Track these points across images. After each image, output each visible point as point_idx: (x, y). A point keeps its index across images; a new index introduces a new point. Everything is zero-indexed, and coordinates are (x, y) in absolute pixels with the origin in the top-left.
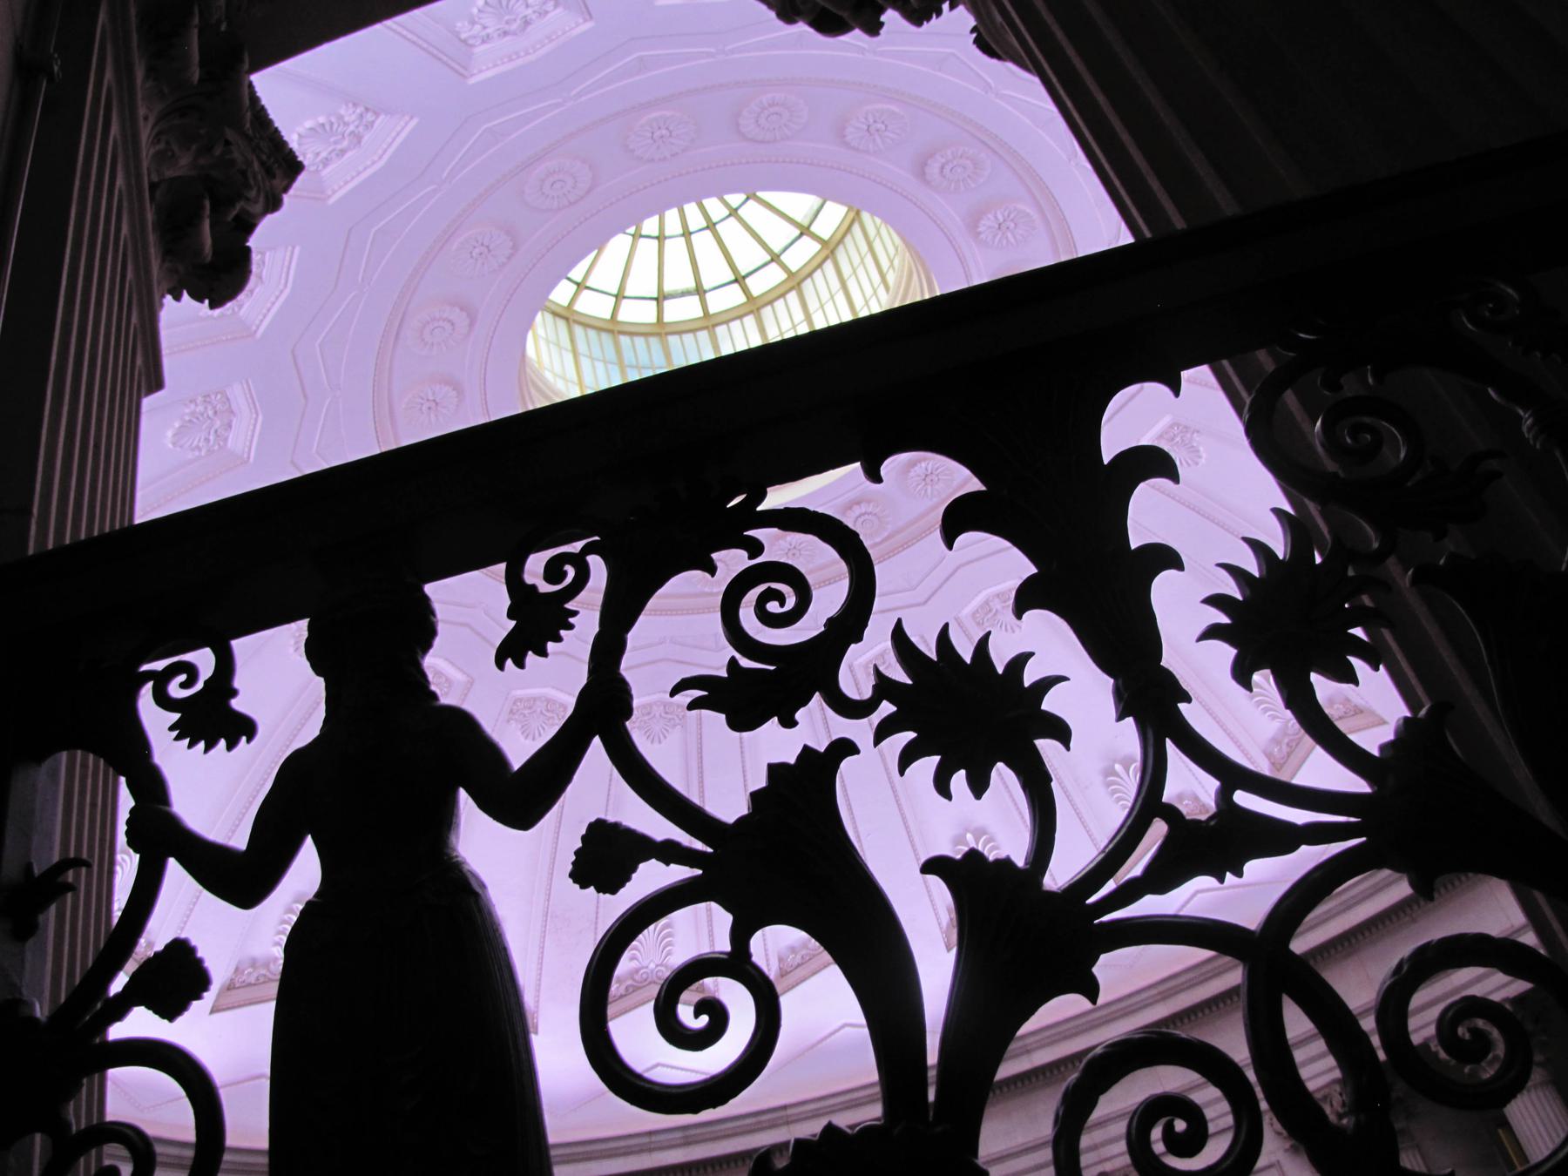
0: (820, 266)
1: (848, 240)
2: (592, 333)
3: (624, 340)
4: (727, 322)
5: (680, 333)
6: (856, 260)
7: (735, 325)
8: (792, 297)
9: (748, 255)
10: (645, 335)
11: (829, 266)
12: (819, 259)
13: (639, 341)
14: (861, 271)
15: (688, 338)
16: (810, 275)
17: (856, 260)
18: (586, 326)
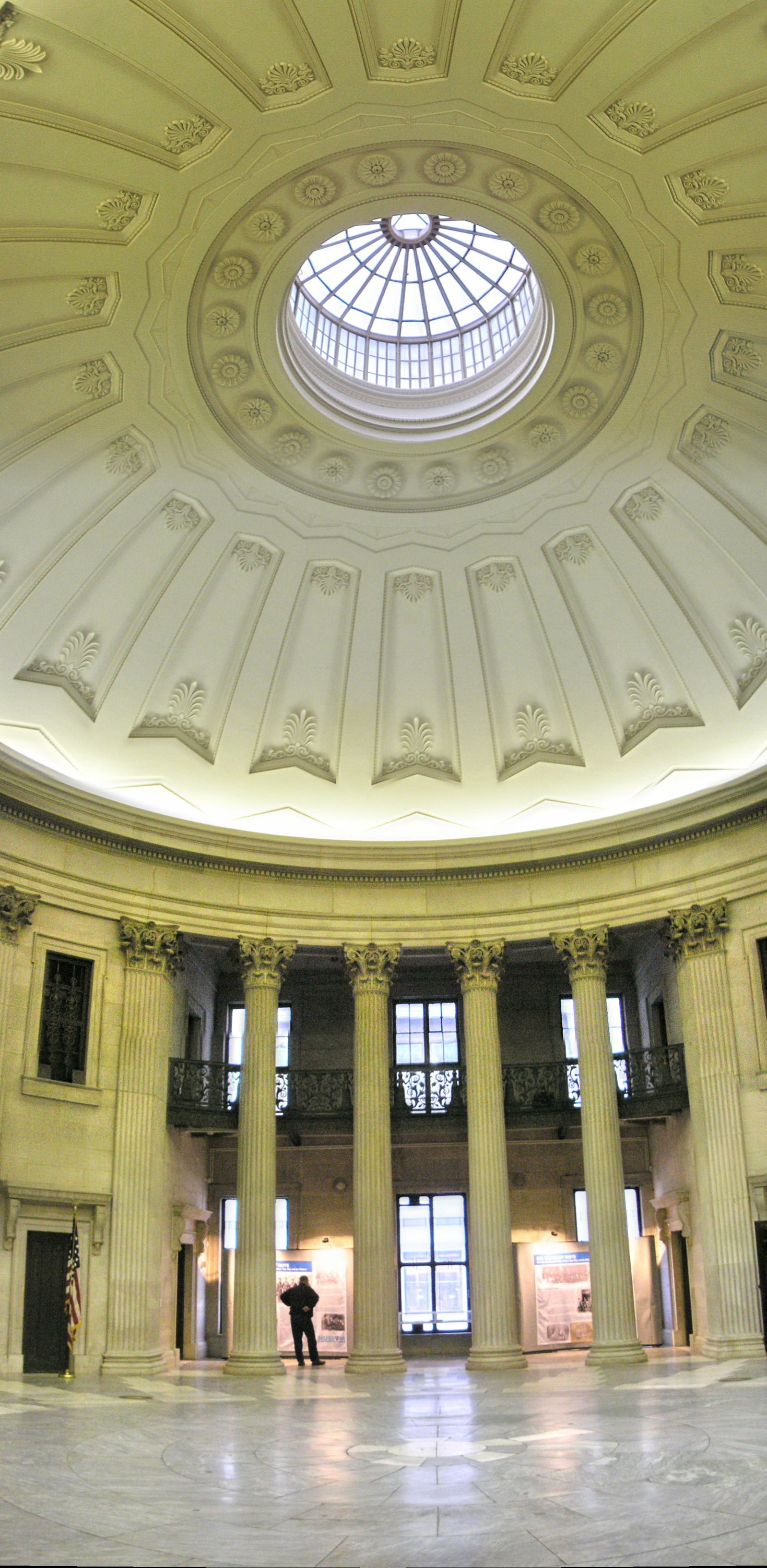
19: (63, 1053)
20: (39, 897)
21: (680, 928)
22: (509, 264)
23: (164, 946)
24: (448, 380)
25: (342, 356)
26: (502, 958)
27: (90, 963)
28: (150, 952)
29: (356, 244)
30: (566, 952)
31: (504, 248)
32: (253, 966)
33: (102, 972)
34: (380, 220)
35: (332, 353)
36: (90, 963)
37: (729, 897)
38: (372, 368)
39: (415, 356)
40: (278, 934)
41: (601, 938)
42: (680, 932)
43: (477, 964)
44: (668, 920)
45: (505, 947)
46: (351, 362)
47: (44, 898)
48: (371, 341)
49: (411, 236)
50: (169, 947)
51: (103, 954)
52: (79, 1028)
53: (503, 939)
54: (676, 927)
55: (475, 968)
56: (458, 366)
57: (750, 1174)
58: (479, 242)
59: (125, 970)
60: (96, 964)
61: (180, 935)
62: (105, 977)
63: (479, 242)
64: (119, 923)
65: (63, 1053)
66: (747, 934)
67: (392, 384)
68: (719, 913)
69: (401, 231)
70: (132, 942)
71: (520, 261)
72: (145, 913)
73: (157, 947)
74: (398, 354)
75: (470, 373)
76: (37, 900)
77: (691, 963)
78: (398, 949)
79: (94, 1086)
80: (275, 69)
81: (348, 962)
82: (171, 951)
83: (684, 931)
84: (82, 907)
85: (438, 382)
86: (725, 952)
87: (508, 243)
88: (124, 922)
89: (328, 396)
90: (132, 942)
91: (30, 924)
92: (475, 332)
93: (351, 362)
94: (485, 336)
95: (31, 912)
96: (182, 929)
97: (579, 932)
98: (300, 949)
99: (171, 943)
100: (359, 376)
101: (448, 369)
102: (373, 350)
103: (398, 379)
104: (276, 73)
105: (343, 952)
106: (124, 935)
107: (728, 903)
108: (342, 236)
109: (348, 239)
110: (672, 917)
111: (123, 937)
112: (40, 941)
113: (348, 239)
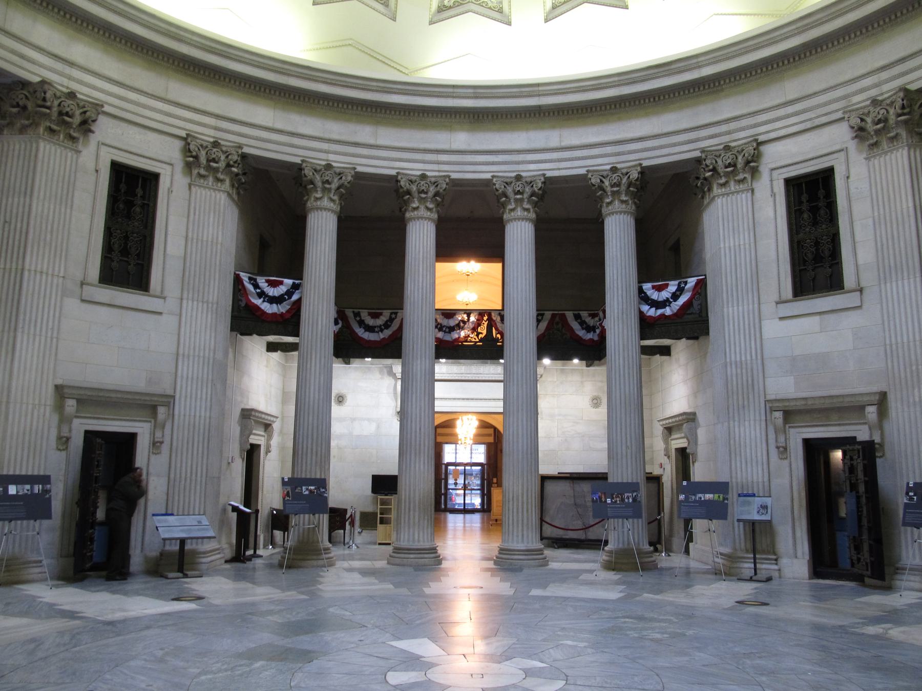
19: (127, 258)
20: (102, 106)
21: (711, 167)
23: (228, 166)
26: (540, 192)
27: (156, 177)
28: (216, 170)
30: (602, 189)
32: (315, 188)
33: (168, 184)
36: (156, 177)
37: (761, 138)
40: (339, 161)
41: (634, 175)
42: (710, 171)
43: (518, 197)
44: (698, 161)
45: (544, 183)
47: (107, 108)
50: (233, 166)
51: (168, 168)
52: (145, 237)
53: (544, 175)
54: (707, 166)
55: (516, 200)
57: (768, 398)
59: (190, 185)
60: (162, 180)
61: (244, 156)
62: (170, 191)
64: (186, 140)
65: (127, 258)
66: (775, 173)
68: (750, 150)
70: (198, 159)
72: (212, 132)
73: (222, 165)
76: (98, 107)
77: (719, 201)
78: (447, 180)
79: (158, 293)
81: (401, 190)
82: (234, 170)
83: (714, 170)
84: (145, 123)
86: (753, 190)
88: (189, 140)
90: (198, 159)
91: (93, 132)
95: (94, 121)
96: (246, 150)
97: (614, 170)
98: (359, 176)
99: (235, 162)
105: (398, 181)
106: (190, 151)
107: (760, 144)
110: (703, 156)
111: (187, 151)
112: (104, 149)
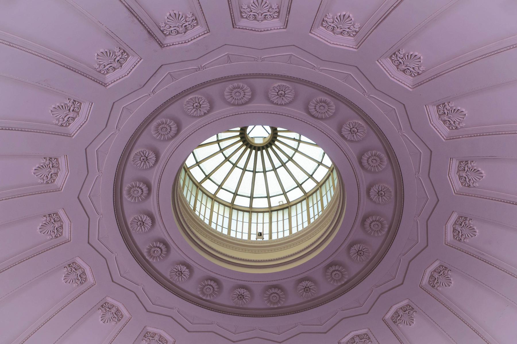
0: (301, 201)
1: (314, 195)
2: (205, 196)
3: (216, 205)
4: (258, 212)
5: (238, 210)
6: (315, 202)
7: (261, 215)
8: (286, 211)
9: (275, 189)
10: (225, 205)
11: (304, 203)
12: (302, 199)
13: (222, 207)
14: (315, 206)
15: (241, 213)
16: (296, 204)
17: (315, 202)
18: (203, 192)
22: (320, 164)
24: (281, 236)
25: (214, 220)
29: (223, 145)
31: (317, 152)
34: (239, 129)
35: (208, 216)
38: (233, 227)
39: (260, 220)
46: (220, 223)
48: (234, 210)
49: (259, 141)
56: (287, 227)
58: (303, 148)
63: (303, 148)
67: (245, 237)
69: (252, 138)
71: (328, 161)
74: (250, 219)
75: (294, 231)
80: (170, 15)
85: (274, 237)
87: (321, 149)
89: (204, 243)
92: (299, 205)
93: (220, 223)
94: (305, 208)
100: (225, 232)
101: (281, 229)
102: (234, 216)
103: (250, 234)
104: (171, 18)
108: (214, 138)
109: (218, 141)
113: (218, 141)
